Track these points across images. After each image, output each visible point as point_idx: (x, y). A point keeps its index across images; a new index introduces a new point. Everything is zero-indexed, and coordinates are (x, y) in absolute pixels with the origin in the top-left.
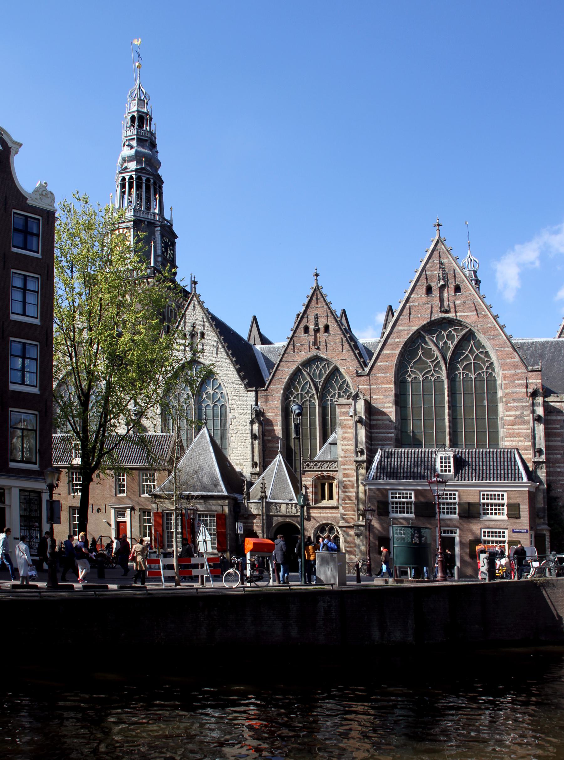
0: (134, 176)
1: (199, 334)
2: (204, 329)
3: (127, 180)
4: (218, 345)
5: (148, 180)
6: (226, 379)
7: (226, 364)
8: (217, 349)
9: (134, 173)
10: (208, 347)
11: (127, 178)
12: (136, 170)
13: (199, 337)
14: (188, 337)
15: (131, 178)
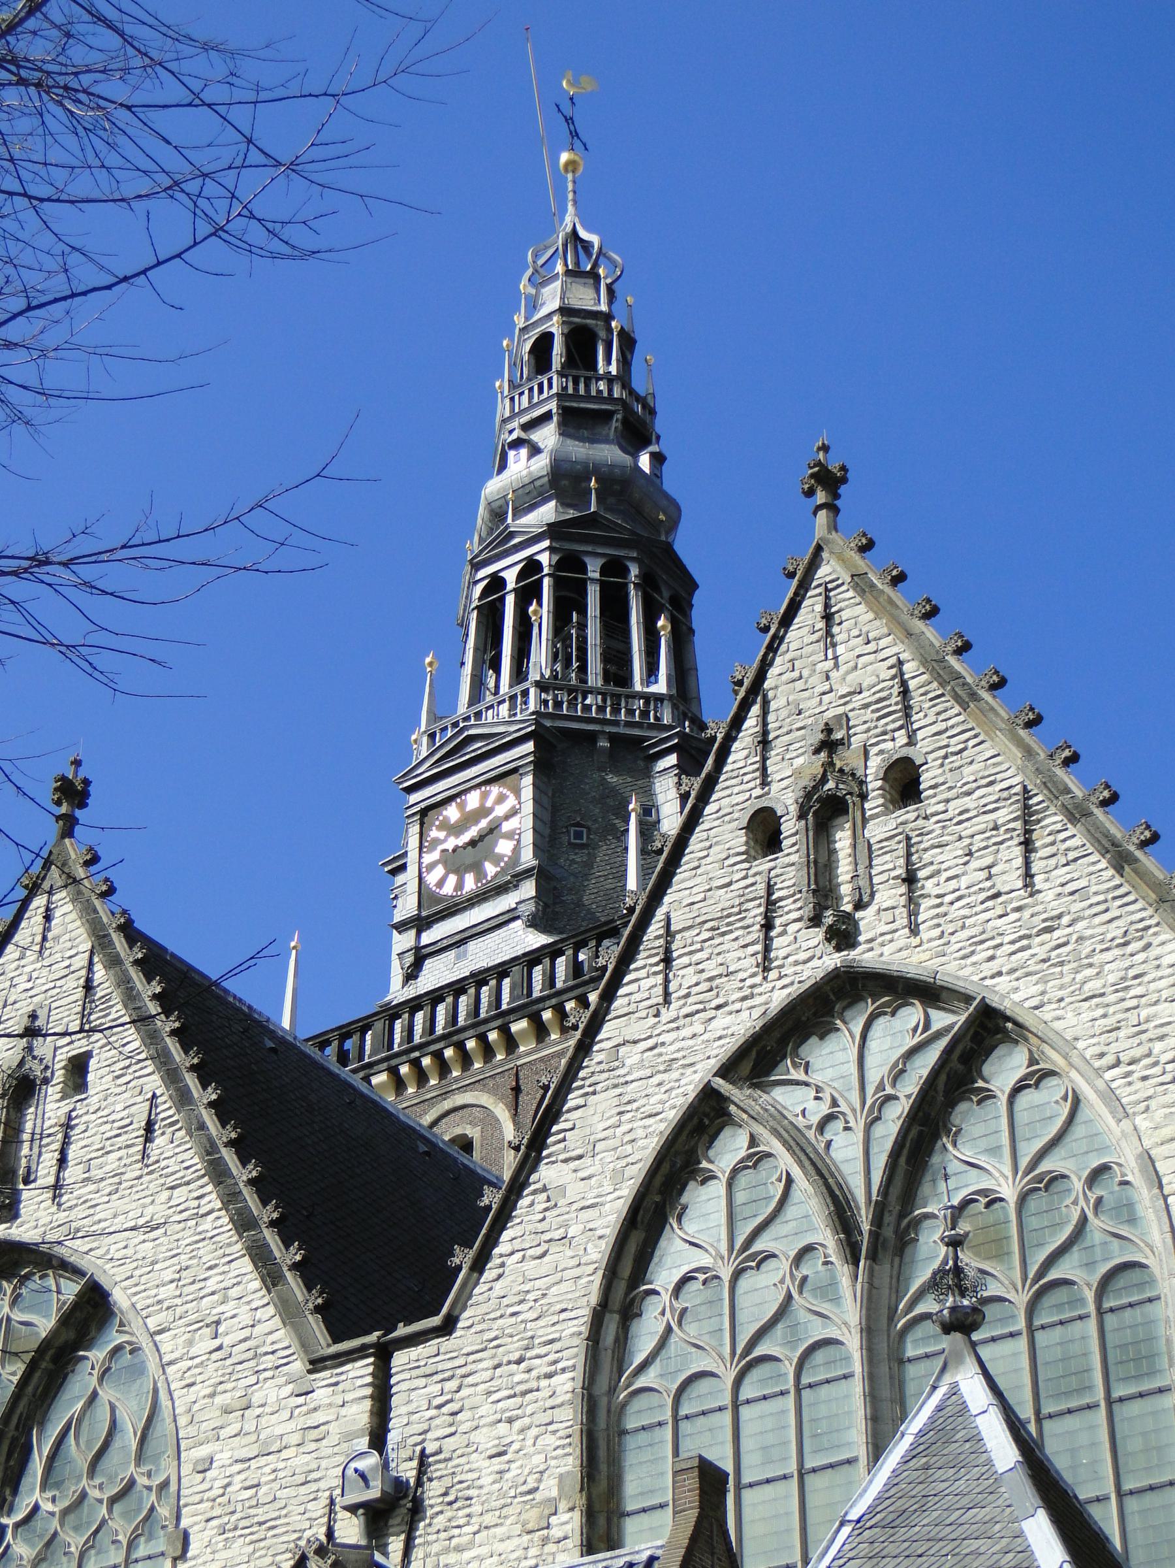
0: (544, 559)
1: (874, 784)
2: (911, 742)
3: (511, 584)
4: (1027, 816)
5: (614, 568)
6: (1123, 1045)
7: (1115, 930)
8: (1028, 845)
9: (546, 543)
10: (958, 849)
11: (511, 577)
12: (554, 531)
13: (874, 804)
14: (789, 826)
15: (532, 566)
